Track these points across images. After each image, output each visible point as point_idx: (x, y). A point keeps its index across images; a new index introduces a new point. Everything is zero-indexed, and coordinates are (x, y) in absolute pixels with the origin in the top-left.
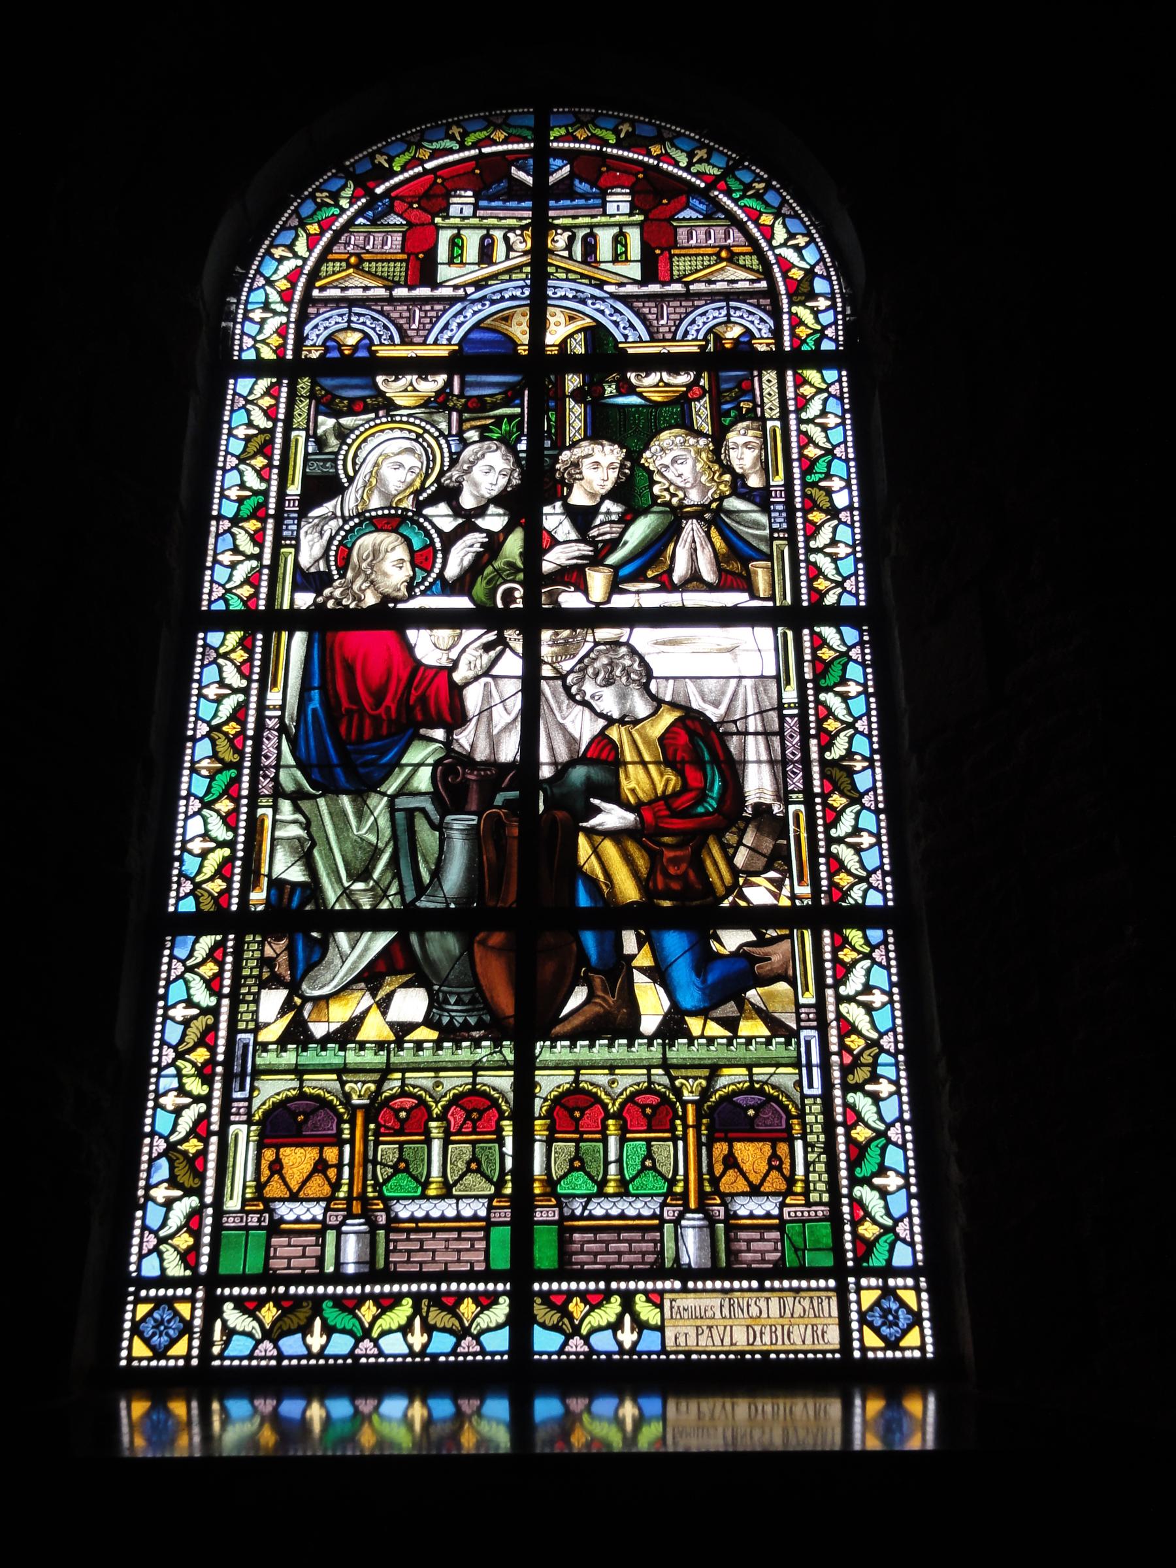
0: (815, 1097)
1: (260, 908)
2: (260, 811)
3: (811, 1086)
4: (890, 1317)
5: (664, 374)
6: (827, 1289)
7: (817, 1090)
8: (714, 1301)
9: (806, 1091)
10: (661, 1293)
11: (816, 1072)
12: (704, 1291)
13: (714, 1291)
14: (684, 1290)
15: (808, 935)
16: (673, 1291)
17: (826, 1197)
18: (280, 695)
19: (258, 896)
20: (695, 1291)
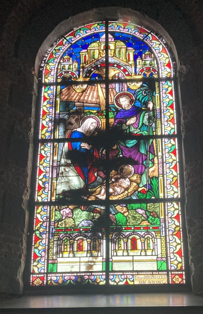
0: (163, 237)
1: (54, 201)
2: (53, 181)
3: (162, 234)
4: (177, 280)
5: (135, 83)
6: (165, 274)
7: (164, 235)
8: (143, 276)
9: (162, 235)
10: (134, 275)
11: (164, 232)
12: (142, 274)
13: (143, 274)
14: (138, 274)
15: (163, 204)
16: (136, 274)
17: (165, 256)
18: (57, 157)
19: (54, 198)
20: (140, 274)
